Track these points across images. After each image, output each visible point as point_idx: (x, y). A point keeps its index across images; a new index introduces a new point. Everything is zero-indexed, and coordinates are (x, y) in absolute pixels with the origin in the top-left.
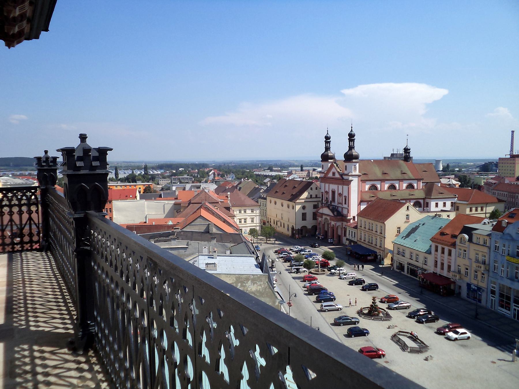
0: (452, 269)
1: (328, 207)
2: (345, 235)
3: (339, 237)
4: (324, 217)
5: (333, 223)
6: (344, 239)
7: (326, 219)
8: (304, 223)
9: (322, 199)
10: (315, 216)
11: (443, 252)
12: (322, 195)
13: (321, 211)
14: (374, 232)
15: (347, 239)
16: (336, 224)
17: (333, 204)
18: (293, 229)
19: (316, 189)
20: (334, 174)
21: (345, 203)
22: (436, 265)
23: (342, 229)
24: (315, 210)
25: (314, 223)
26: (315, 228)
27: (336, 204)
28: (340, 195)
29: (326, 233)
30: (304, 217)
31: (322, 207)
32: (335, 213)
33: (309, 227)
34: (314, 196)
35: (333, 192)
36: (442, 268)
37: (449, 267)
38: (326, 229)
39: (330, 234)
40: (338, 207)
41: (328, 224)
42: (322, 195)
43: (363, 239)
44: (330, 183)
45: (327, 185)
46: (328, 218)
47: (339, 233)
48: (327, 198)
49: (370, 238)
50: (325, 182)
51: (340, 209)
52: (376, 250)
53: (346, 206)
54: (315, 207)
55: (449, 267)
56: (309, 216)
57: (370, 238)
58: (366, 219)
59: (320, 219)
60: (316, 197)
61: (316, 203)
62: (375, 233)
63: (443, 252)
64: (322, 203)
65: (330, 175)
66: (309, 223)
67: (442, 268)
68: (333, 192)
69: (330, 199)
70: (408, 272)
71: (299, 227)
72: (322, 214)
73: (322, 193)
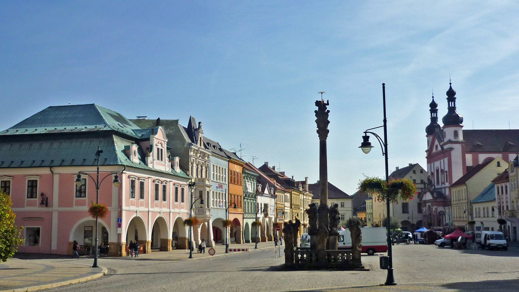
4: (428, 204)
13: (424, 199)
16: (436, 209)
20: (437, 146)
34: (418, 181)
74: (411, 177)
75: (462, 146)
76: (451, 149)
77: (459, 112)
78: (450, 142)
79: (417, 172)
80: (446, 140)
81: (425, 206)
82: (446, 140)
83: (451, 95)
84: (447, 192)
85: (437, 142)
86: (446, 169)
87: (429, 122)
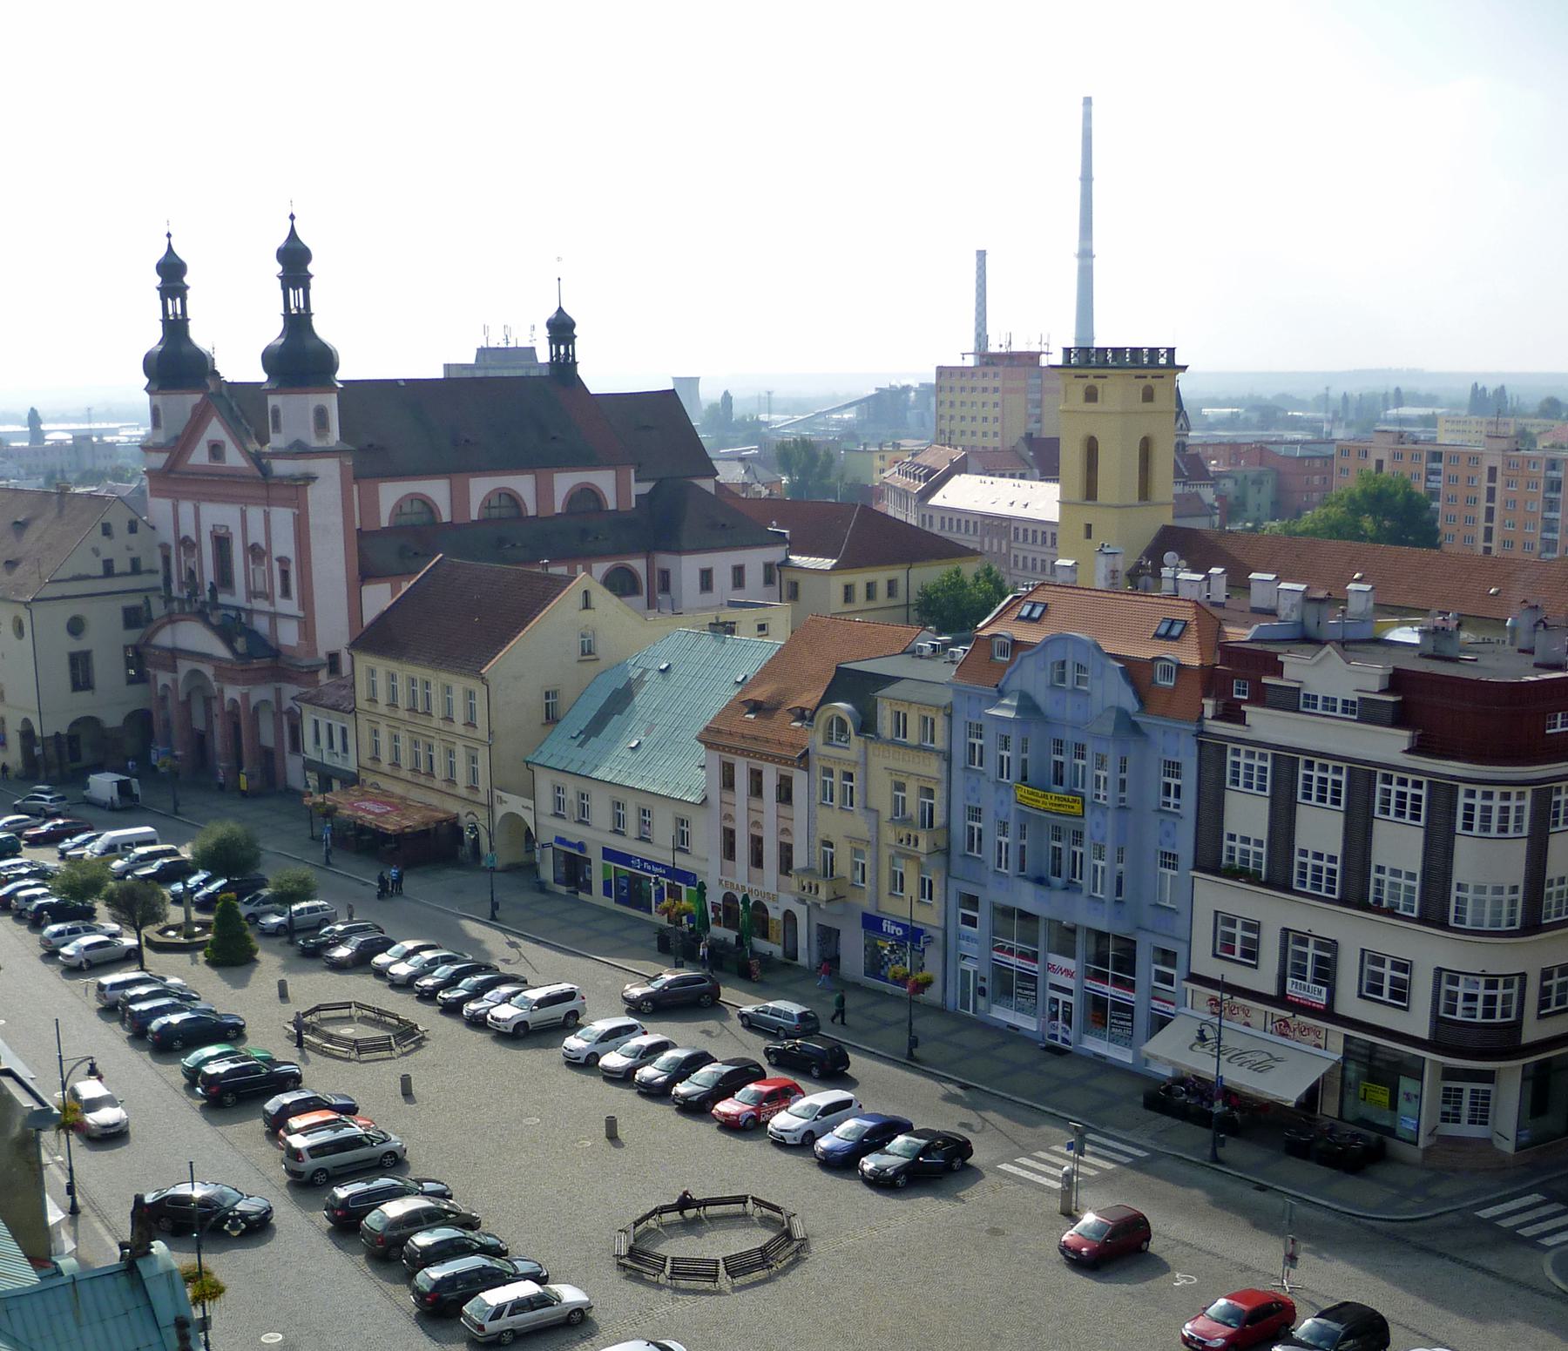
0: (799, 860)
1: (202, 615)
2: (296, 746)
3: (268, 758)
4: (185, 666)
5: (232, 692)
6: (293, 765)
7: (195, 673)
8: (83, 704)
9: (168, 580)
10: (139, 661)
11: (757, 790)
12: (166, 560)
14: (436, 722)
15: (309, 765)
16: (246, 697)
17: (223, 598)
18: (27, 735)
19: (133, 528)
20: (216, 450)
21: (286, 593)
22: (729, 851)
23: (277, 714)
24: (133, 636)
25: (135, 698)
26: (141, 721)
27: (238, 597)
28: (256, 553)
29: (200, 742)
30: (81, 672)
31: (171, 619)
32: (240, 644)
33: (113, 718)
34: (122, 565)
35: (222, 543)
36: (757, 860)
37: (786, 851)
38: (199, 724)
39: (218, 744)
40: (250, 612)
41: (208, 701)
42: (166, 560)
43: (385, 756)
44: (199, 498)
45: (186, 508)
46: (208, 670)
47: (268, 739)
48: (192, 573)
49: (421, 750)
50: (176, 497)
51: (261, 625)
52: (454, 807)
53: (291, 606)
54: (133, 618)
55: (786, 851)
56: (109, 668)
57: (421, 750)
58: (393, 666)
59: (163, 678)
60: (136, 568)
61: (135, 601)
62: (441, 724)
63: (757, 790)
64: (169, 599)
65: (199, 456)
66: (111, 701)
67: (757, 860)
68: (222, 543)
69: (209, 575)
70: (607, 892)
71: (58, 724)
72: (175, 654)
73: (165, 547)
74: (96, 552)
75: (342, 465)
76: (310, 478)
77: (325, 328)
78: (299, 450)
79: (115, 530)
80: (277, 441)
81: (174, 670)
82: (277, 441)
83: (294, 262)
84: (288, 635)
85: (215, 430)
86: (284, 546)
87: (152, 337)
